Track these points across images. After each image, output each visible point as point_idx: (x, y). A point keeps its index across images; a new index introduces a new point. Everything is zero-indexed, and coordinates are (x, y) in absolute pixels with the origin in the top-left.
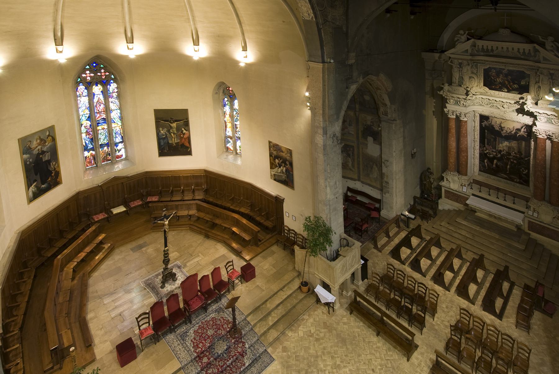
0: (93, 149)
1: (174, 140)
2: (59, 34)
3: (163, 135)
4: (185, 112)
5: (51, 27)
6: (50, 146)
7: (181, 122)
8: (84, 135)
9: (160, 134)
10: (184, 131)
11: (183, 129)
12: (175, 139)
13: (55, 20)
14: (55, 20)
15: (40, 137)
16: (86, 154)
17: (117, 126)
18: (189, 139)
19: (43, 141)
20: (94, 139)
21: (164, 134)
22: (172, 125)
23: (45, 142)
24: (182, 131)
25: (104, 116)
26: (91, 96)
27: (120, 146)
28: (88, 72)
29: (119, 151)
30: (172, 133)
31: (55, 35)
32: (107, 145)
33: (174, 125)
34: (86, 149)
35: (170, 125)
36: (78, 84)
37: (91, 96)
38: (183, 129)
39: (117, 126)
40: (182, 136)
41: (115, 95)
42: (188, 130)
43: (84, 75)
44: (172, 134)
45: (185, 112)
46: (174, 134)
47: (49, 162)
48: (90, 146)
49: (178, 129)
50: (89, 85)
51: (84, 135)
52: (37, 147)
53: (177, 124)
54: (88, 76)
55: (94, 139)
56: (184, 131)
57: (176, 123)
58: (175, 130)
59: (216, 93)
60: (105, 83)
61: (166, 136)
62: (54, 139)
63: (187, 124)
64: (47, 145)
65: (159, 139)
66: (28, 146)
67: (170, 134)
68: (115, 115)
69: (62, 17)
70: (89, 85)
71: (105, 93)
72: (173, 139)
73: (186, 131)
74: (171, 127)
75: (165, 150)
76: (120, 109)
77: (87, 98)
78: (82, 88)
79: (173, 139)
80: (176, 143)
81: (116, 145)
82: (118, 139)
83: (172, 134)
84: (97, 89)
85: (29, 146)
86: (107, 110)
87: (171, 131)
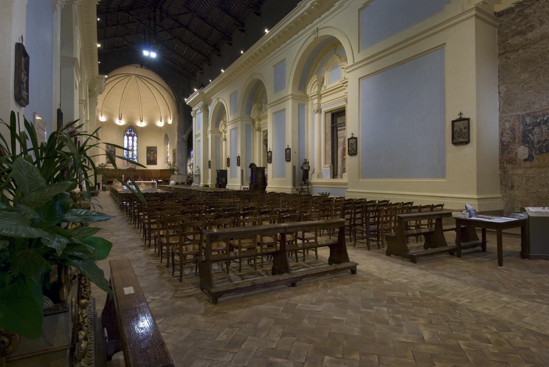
1: (152, 159)
2: (120, 117)
4: (156, 147)
5: (118, 114)
8: (125, 153)
13: (120, 112)
14: (120, 112)
17: (135, 153)
25: (131, 148)
26: (128, 140)
31: (119, 117)
32: (131, 158)
33: (152, 153)
37: (128, 140)
39: (135, 153)
42: (156, 155)
45: (156, 147)
49: (153, 154)
50: (128, 136)
54: (128, 133)
63: (156, 152)
65: (147, 158)
68: (135, 148)
69: (122, 111)
70: (128, 136)
71: (133, 140)
74: (151, 154)
76: (137, 146)
78: (126, 137)
82: (135, 158)
84: (130, 138)
86: (133, 146)
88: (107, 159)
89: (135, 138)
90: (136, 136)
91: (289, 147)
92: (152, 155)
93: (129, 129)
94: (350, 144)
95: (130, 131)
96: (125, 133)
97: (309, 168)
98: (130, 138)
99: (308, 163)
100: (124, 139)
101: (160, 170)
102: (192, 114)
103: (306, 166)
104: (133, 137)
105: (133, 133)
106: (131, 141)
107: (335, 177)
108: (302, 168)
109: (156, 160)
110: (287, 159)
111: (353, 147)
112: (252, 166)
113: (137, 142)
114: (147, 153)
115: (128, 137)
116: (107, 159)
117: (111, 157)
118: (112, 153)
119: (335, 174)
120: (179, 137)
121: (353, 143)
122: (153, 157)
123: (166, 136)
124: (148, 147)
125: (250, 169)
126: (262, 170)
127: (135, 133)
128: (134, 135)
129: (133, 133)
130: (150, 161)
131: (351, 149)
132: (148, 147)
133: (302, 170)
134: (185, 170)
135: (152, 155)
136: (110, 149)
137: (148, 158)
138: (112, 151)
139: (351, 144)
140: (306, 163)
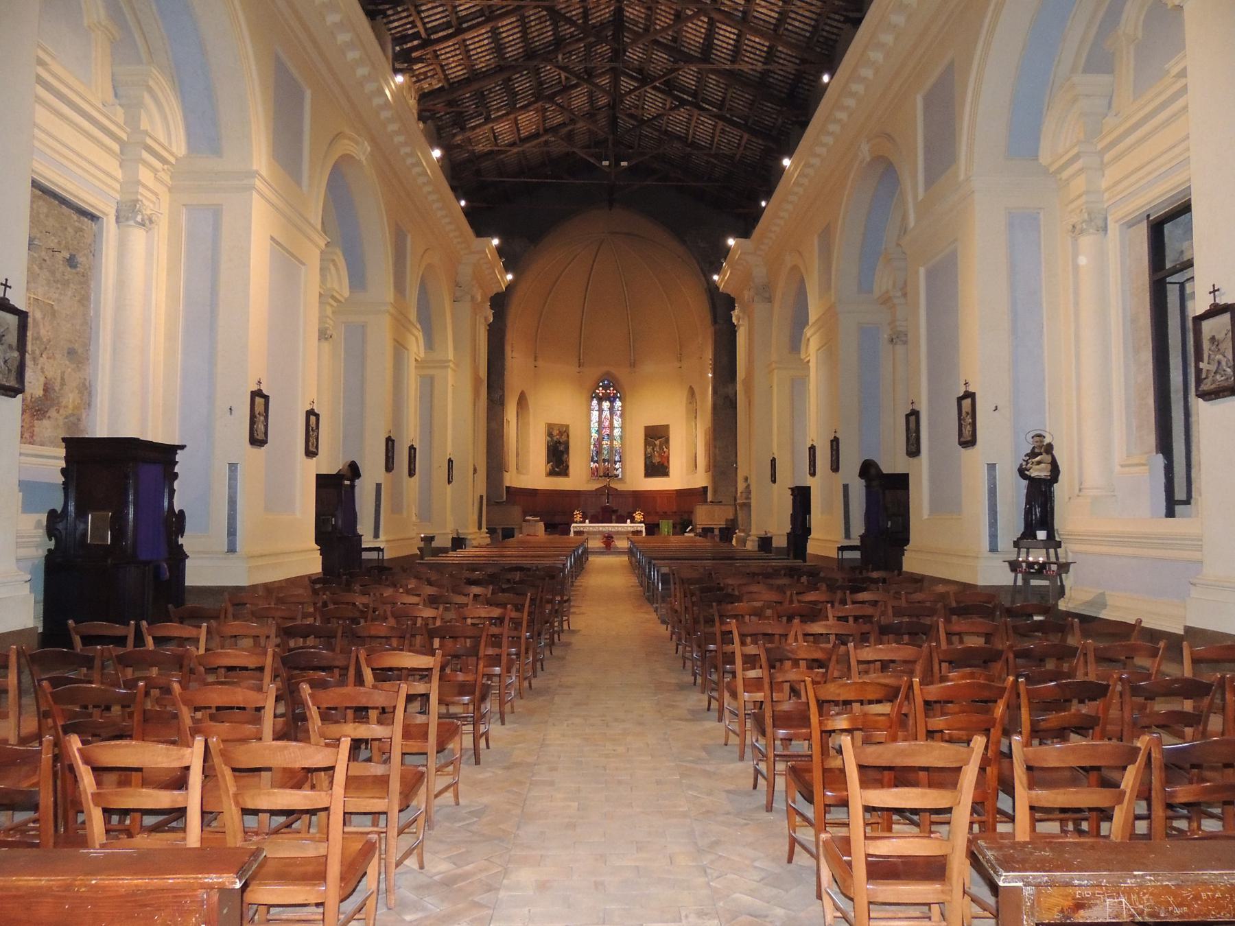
0: (597, 462)
1: (656, 460)
4: (667, 427)
10: (665, 449)
16: (592, 465)
19: (561, 433)
20: (598, 453)
26: (601, 411)
27: (618, 465)
28: (601, 389)
29: (617, 470)
33: (657, 442)
34: (592, 460)
36: (592, 398)
37: (601, 411)
41: (619, 413)
42: (668, 448)
43: (598, 391)
45: (667, 427)
47: (562, 452)
48: (596, 459)
49: (661, 448)
50: (600, 400)
51: (592, 447)
54: (600, 391)
55: (598, 453)
56: (665, 449)
59: (690, 403)
60: (612, 402)
62: (568, 436)
63: (667, 441)
65: (646, 458)
68: (617, 432)
70: (600, 400)
71: (611, 409)
74: (655, 445)
77: (597, 413)
78: (595, 402)
81: (615, 462)
82: (617, 458)
84: (606, 405)
86: (612, 427)
89: (618, 404)
90: (620, 399)
91: (971, 389)
92: (657, 449)
93: (603, 381)
94: (1206, 345)
95: (606, 387)
96: (594, 392)
97: (1055, 469)
98: (606, 405)
99: (1049, 449)
100: (590, 409)
102: (734, 320)
103: (1039, 463)
104: (612, 402)
105: (611, 391)
106: (606, 413)
107: (1178, 508)
108: (1022, 472)
109: (666, 464)
110: (962, 440)
111: (1219, 357)
112: (868, 470)
113: (622, 416)
114: (647, 443)
115: (600, 404)
117: (558, 456)
118: (562, 448)
119: (1180, 494)
120: (715, 392)
121: (1219, 337)
122: (661, 456)
123: (692, 392)
125: (863, 482)
126: (900, 482)
127: (618, 392)
128: (615, 397)
129: (611, 391)
130: (653, 465)
131: (1213, 367)
133: (1025, 483)
134: (734, 490)
135: (657, 449)
136: (555, 439)
137: (648, 458)
138: (560, 442)
139: (1213, 339)
140: (1042, 449)
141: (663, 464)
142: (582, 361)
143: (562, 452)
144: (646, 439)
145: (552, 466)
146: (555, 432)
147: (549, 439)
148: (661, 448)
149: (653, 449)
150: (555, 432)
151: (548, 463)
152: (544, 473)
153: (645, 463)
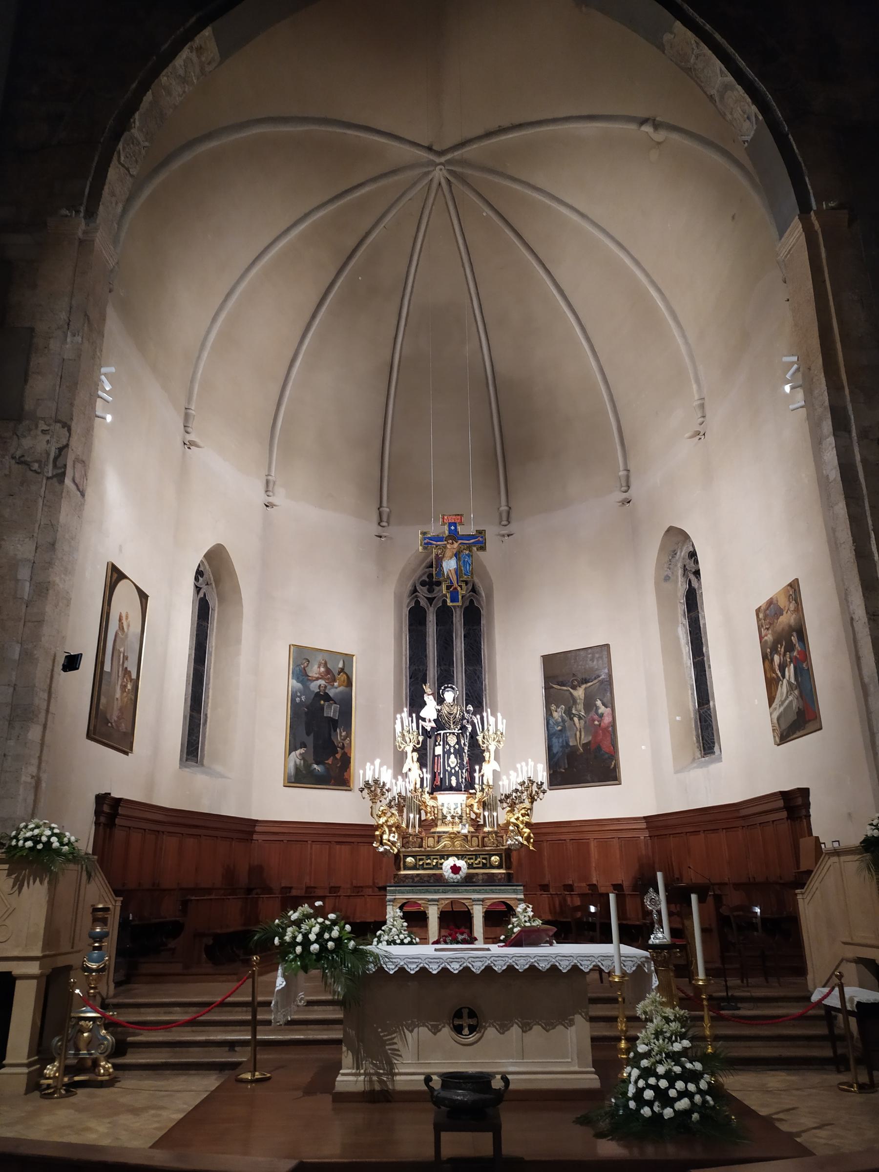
1: (579, 737)
3: (557, 724)
6: (341, 692)
7: (595, 682)
9: (551, 722)
10: (602, 709)
11: (599, 703)
12: (583, 733)
15: (326, 664)
18: (611, 732)
19: (329, 675)
21: (560, 720)
22: (575, 693)
23: (335, 681)
24: (597, 708)
30: (574, 715)
33: (579, 693)
35: (571, 694)
38: (599, 703)
40: (596, 723)
42: (610, 704)
44: (576, 719)
46: (580, 718)
47: (333, 724)
49: (589, 705)
52: (317, 679)
53: (585, 689)
56: (602, 709)
57: (584, 686)
58: (581, 707)
61: (564, 728)
62: (349, 683)
64: (336, 688)
66: (302, 666)
67: (572, 719)
72: (578, 733)
73: (606, 707)
75: (560, 768)
79: (578, 733)
80: (585, 746)
83: (576, 719)
85: (304, 669)
87: (574, 712)
88: (296, 756)
101: (646, 819)
109: (606, 746)
114: (550, 699)
116: (296, 756)
118: (331, 711)
124: (549, 661)
132: (549, 661)
136: (314, 686)
138: (327, 697)
141: (599, 748)
142: (386, 510)
143: (333, 724)
144: (547, 688)
145: (303, 757)
146: (315, 670)
147: (294, 683)
148: (589, 705)
149: (568, 712)
150: (315, 670)
151: (292, 747)
152: (279, 777)
153: (550, 748)
